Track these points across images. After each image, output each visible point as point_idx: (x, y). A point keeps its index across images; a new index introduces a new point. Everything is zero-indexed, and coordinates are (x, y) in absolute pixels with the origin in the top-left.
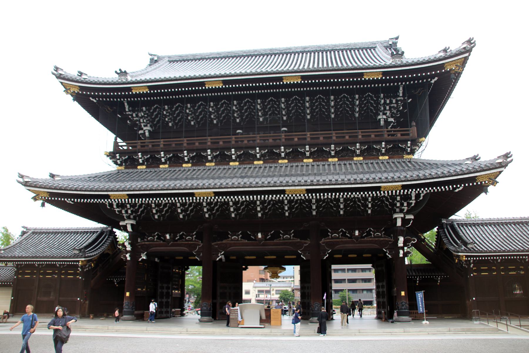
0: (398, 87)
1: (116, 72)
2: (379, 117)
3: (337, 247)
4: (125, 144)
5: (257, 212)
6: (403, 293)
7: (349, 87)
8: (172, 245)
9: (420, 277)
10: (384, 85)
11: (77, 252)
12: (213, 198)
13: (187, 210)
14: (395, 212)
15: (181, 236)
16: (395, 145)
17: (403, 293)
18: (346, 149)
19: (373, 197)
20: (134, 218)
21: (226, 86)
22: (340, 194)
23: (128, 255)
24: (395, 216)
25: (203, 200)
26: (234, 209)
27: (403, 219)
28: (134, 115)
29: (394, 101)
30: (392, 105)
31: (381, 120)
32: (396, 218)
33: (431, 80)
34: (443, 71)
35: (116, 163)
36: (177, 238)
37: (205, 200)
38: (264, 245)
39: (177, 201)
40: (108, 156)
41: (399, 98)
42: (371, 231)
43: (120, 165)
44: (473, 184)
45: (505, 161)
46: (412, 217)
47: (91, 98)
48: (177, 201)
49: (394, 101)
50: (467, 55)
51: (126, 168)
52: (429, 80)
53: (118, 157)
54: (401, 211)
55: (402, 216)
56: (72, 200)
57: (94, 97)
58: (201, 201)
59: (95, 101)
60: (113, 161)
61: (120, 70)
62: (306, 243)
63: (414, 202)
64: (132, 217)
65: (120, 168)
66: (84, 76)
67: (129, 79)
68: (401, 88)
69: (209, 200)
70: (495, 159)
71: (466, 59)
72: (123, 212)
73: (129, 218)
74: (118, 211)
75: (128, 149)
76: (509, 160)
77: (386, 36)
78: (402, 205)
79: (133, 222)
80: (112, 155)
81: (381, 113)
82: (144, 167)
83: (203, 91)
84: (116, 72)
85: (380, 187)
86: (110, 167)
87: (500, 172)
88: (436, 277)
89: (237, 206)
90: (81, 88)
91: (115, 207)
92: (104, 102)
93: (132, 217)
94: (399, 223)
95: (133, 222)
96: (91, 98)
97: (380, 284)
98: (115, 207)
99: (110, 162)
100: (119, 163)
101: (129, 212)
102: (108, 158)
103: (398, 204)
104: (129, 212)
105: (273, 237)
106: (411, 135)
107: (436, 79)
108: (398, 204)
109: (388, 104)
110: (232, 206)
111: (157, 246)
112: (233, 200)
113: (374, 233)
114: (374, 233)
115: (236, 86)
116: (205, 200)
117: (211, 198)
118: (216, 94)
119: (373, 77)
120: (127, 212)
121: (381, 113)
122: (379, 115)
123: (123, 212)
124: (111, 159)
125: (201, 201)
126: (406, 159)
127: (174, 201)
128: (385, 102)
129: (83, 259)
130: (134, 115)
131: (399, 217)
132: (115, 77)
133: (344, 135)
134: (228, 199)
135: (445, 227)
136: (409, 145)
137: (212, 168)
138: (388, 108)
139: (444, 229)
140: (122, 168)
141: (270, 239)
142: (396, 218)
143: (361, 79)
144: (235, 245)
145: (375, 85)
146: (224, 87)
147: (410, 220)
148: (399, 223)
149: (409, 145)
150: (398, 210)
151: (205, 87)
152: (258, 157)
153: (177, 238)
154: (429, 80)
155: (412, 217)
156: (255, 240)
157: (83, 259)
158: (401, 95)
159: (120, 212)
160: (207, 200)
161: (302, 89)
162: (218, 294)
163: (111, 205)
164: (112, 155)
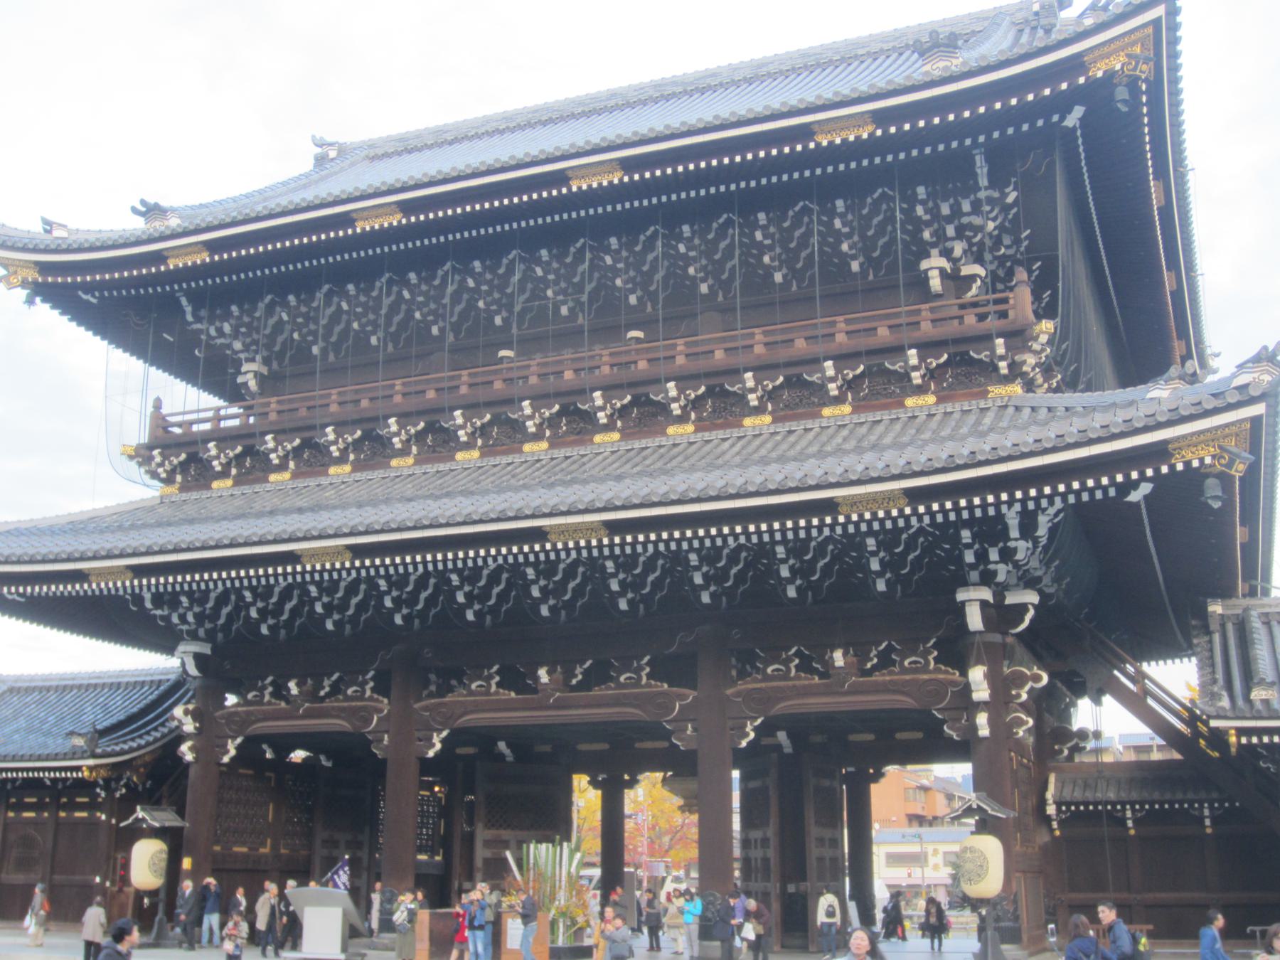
1: (134, 210)
3: (780, 708)
4: (235, 410)
5: (870, 576)
7: (641, 203)
8: (309, 715)
9: (1132, 804)
10: (941, 147)
11: (79, 742)
13: (485, 595)
14: (965, 583)
15: (336, 689)
16: (714, 387)
18: (795, 382)
21: (631, 178)
26: (882, 562)
33: (1062, 119)
34: (1082, 80)
35: (154, 475)
36: (322, 693)
38: (559, 705)
40: (131, 457)
42: (894, 649)
43: (169, 481)
47: (80, 293)
51: (184, 488)
52: (1056, 118)
53: (158, 459)
54: (987, 579)
55: (986, 594)
59: (94, 301)
60: (147, 472)
61: (143, 202)
62: (682, 697)
64: (201, 632)
66: (57, 233)
67: (174, 222)
74: (162, 618)
75: (245, 425)
78: (982, 557)
79: (206, 649)
80: (142, 455)
82: (544, 445)
84: (134, 210)
86: (140, 489)
88: (1191, 805)
89: (892, 554)
90: (44, 268)
91: (148, 605)
92: (137, 296)
93: (201, 632)
94: (975, 620)
96: (80, 293)
97: (756, 834)
98: (148, 605)
100: (164, 475)
101: (190, 618)
102: (133, 464)
104: (190, 618)
105: (885, 661)
106: (1011, 314)
107: (1078, 111)
108: (969, 557)
110: (874, 554)
111: (267, 717)
115: (642, 177)
118: (532, 222)
119: (830, 137)
120: (183, 618)
122: (928, 256)
124: (140, 464)
126: (994, 399)
129: (91, 762)
132: (137, 225)
133: (490, 378)
135: (1214, 626)
136: (1001, 350)
137: (406, 472)
139: (1209, 633)
140: (172, 489)
141: (582, 686)
143: (805, 147)
144: (477, 708)
145: (748, 184)
146: (404, 221)
147: (1023, 608)
148: (975, 620)
149: (1001, 350)
151: (570, 189)
152: (464, 439)
153: (322, 693)
154: (1056, 118)
156: (535, 691)
157: (91, 762)
161: (645, 203)
162: (479, 863)
163: (138, 599)
164: (142, 455)
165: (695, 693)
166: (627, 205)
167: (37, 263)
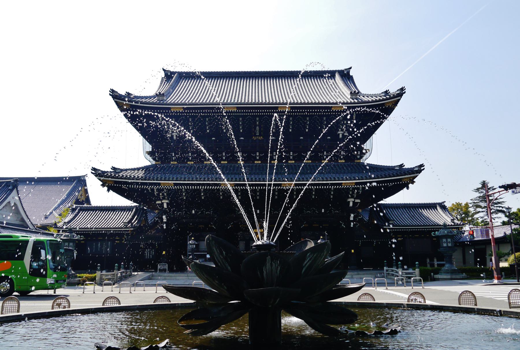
2: (339, 132)
6: (353, 251)
14: (349, 198)
17: (353, 251)
20: (168, 199)
23: (165, 225)
24: (349, 200)
27: (354, 202)
32: (349, 202)
35: (154, 159)
40: (149, 154)
45: (420, 169)
46: (359, 201)
50: (399, 98)
55: (353, 200)
63: (361, 191)
64: (166, 198)
65: (157, 163)
70: (414, 168)
71: (399, 100)
72: (161, 194)
73: (164, 198)
76: (422, 168)
77: (342, 67)
79: (167, 201)
81: (340, 130)
85: (342, 183)
87: (417, 176)
93: (166, 198)
94: (351, 204)
95: (167, 201)
99: (150, 158)
101: (165, 194)
103: (351, 193)
108: (351, 193)
109: (345, 124)
113: (334, 211)
114: (334, 211)
120: (163, 194)
121: (340, 130)
123: (161, 194)
126: (357, 163)
128: (344, 122)
131: (351, 201)
138: (345, 126)
142: (349, 202)
147: (358, 203)
148: (351, 204)
155: (359, 201)
159: (158, 194)
163: (153, 190)
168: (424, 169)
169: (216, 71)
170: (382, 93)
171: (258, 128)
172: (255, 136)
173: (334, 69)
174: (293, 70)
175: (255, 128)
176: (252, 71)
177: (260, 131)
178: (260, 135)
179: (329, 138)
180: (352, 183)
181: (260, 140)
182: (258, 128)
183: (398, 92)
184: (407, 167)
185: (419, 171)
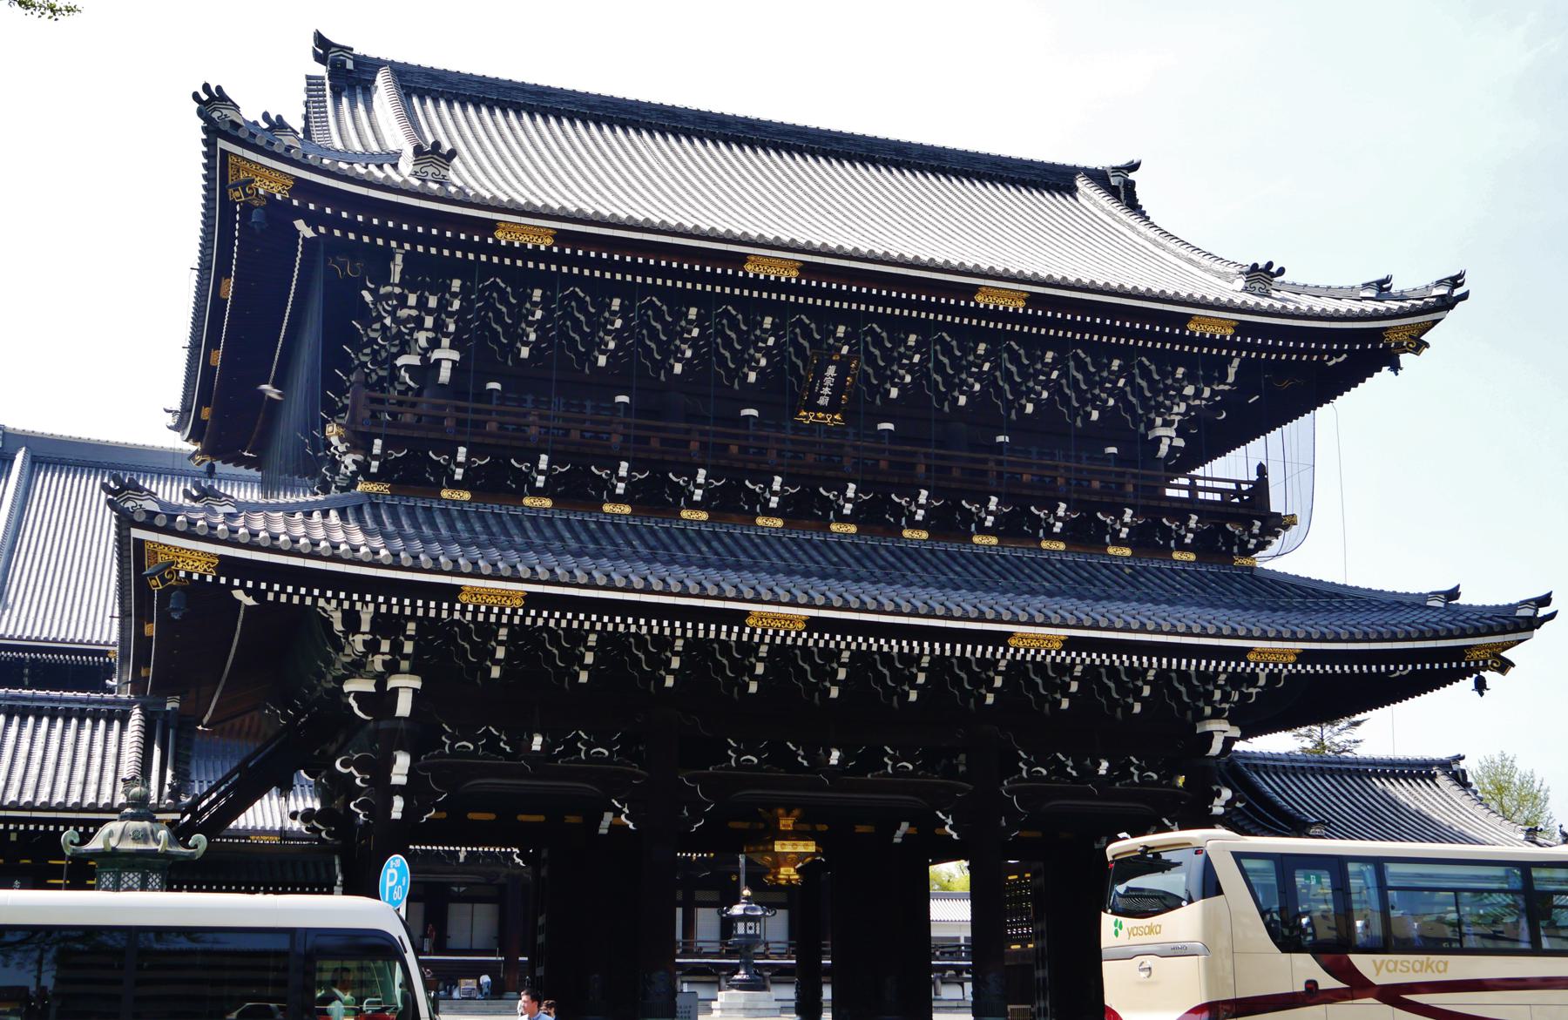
0: (1229, 359)
12: (805, 635)
19: (1160, 671)
22: (1218, 664)
23: (398, 803)
24: (1212, 726)
25: (762, 637)
28: (412, 300)
29: (1207, 393)
30: (1197, 402)
31: (1166, 441)
33: (1330, 359)
37: (767, 639)
39: (678, 632)
41: (1222, 387)
44: (1459, 665)
48: (678, 632)
49: (1207, 393)
56: (250, 584)
57: (312, 221)
58: (756, 639)
68: (1236, 362)
69: (778, 640)
76: (1543, 612)
79: (416, 683)
83: (734, 281)
95: (416, 683)
103: (1218, 695)
104: (408, 648)
108: (1218, 695)
112: (854, 646)
116: (767, 639)
117: (514, 611)
123: (385, 646)
125: (756, 639)
126: (1243, 568)
127: (667, 632)
130: (412, 300)
134: (838, 644)
149: (1256, 530)
150: (1208, 710)
158: (1231, 379)
160: (773, 638)
165: (971, 787)
166: (1000, 326)
167: (297, 179)
168: (1552, 616)
169: (569, 86)
170: (1366, 286)
171: (831, 371)
172: (813, 406)
173: (1070, 162)
174: (904, 138)
175: (820, 375)
176: (728, 112)
177: (838, 387)
178: (831, 408)
179: (1113, 450)
180: (1284, 653)
181: (829, 430)
182: (831, 371)
183: (1443, 291)
184: (1477, 601)
185: (1533, 624)
